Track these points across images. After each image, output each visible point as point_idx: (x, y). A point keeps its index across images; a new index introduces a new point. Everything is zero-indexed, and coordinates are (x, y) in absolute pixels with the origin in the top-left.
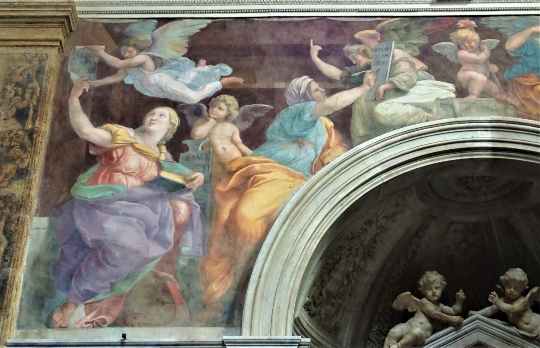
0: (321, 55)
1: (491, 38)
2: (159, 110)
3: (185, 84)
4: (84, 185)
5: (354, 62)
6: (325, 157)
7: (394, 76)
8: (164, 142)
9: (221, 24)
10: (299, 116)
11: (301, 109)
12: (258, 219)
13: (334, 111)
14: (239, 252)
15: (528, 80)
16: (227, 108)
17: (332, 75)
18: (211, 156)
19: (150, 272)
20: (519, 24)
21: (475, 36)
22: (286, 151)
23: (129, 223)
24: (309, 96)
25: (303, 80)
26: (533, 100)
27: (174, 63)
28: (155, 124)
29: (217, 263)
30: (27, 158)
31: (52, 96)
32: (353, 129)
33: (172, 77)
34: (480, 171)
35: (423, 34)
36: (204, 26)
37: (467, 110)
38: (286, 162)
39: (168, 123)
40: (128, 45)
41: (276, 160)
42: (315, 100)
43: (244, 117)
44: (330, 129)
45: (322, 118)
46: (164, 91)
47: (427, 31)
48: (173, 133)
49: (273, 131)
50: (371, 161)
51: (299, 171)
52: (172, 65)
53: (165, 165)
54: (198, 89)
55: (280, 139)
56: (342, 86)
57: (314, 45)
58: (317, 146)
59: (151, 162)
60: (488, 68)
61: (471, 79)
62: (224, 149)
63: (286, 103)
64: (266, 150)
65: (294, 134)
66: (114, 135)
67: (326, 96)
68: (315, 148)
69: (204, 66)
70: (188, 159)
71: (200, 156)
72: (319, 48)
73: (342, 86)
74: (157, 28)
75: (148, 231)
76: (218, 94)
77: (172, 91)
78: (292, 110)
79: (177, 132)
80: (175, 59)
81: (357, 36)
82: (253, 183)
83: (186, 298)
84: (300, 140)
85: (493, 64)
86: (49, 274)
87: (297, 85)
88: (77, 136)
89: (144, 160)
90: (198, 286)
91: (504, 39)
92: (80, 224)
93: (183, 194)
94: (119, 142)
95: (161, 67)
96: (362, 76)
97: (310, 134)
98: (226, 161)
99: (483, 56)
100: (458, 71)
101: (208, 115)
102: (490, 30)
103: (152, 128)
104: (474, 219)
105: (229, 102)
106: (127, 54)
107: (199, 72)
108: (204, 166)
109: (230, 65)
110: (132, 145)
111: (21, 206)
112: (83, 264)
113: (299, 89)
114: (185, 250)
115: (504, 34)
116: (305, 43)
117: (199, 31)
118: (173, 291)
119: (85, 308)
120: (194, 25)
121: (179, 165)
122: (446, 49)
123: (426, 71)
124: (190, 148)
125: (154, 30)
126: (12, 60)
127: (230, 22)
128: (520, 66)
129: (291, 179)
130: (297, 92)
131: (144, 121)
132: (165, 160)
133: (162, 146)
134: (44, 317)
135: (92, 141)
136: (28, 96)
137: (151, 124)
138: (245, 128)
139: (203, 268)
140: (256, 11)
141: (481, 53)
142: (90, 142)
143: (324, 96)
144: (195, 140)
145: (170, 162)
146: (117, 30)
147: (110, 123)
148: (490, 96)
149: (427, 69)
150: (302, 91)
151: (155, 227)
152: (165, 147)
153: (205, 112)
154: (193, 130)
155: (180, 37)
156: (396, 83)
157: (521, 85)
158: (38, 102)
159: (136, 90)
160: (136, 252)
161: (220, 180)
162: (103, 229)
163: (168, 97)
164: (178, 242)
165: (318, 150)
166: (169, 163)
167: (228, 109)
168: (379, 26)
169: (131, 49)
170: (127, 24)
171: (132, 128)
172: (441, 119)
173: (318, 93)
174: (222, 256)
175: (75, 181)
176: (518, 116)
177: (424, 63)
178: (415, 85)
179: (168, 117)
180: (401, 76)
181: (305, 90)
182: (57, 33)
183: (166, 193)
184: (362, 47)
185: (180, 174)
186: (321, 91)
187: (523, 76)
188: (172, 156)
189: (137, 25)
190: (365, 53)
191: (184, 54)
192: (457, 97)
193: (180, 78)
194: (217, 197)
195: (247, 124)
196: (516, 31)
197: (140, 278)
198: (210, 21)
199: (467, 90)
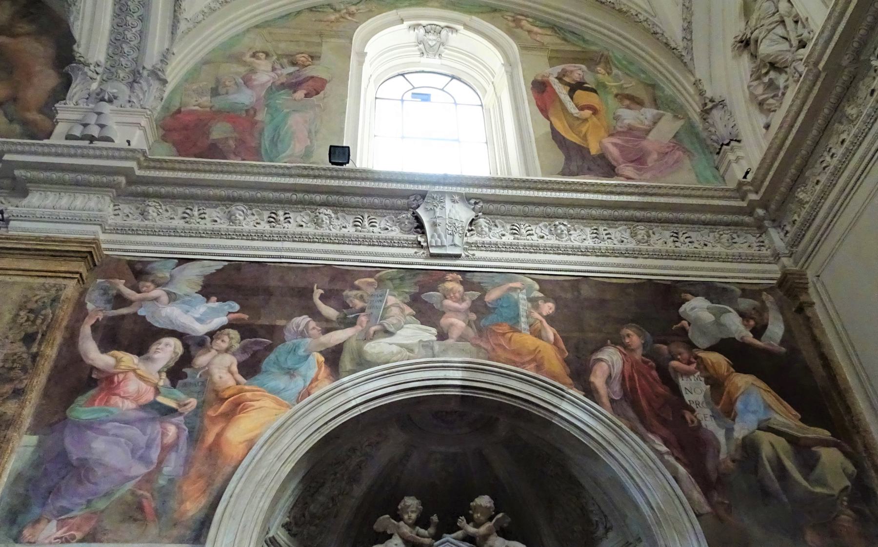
0: (322, 298)
2: (165, 340)
3: (194, 318)
4: (81, 406)
5: (351, 306)
6: (312, 388)
7: (385, 319)
8: (165, 370)
12: (240, 443)
14: (218, 473)
19: (130, 490)
20: (498, 279)
21: (460, 288)
23: (118, 444)
26: (503, 345)
27: (187, 298)
29: (194, 483)
30: (26, 379)
31: (64, 323)
32: (341, 364)
34: (453, 406)
35: (416, 284)
36: (220, 267)
37: (444, 352)
38: (275, 392)
40: (147, 281)
43: (244, 349)
45: (315, 353)
46: (173, 324)
47: (419, 281)
49: (267, 363)
50: (352, 393)
51: (286, 400)
53: (162, 390)
56: (338, 326)
57: (317, 288)
59: (149, 387)
61: (452, 325)
62: (221, 378)
65: (286, 366)
66: (118, 361)
72: (321, 291)
73: (338, 326)
75: (133, 452)
76: (223, 328)
81: (357, 282)
82: (243, 409)
83: (158, 514)
86: (28, 491)
88: (82, 360)
89: (143, 386)
90: (173, 504)
91: (484, 292)
92: (69, 443)
93: (174, 417)
94: (123, 367)
96: (356, 317)
98: (220, 389)
99: (465, 305)
102: (473, 283)
103: (156, 356)
104: (452, 450)
105: (232, 336)
106: (144, 289)
109: (239, 304)
110: (134, 371)
111: (10, 425)
112: (64, 481)
113: (298, 326)
114: (166, 470)
116: (310, 287)
118: (148, 509)
119: (57, 526)
121: (175, 391)
124: (188, 376)
126: (31, 288)
127: (244, 265)
128: (496, 316)
129: (278, 407)
134: (15, 531)
135: (97, 366)
136: (39, 321)
139: (180, 487)
140: (268, 257)
142: (95, 367)
146: (139, 267)
147: (118, 350)
148: (466, 340)
150: (301, 328)
151: (143, 448)
153: (209, 344)
155: (197, 275)
156: (386, 325)
157: (494, 331)
158: (48, 327)
160: (120, 470)
161: (211, 406)
162: (90, 448)
163: (176, 329)
164: (161, 462)
168: (378, 275)
169: (148, 284)
170: (149, 262)
173: (315, 331)
174: (200, 476)
175: (72, 402)
176: (489, 359)
178: (402, 327)
180: (390, 319)
182: (81, 267)
183: (158, 416)
184: (359, 293)
185: (176, 400)
187: (497, 325)
189: (159, 264)
190: (361, 298)
192: (437, 340)
194: (206, 422)
196: (496, 286)
197: (117, 495)
198: (226, 263)
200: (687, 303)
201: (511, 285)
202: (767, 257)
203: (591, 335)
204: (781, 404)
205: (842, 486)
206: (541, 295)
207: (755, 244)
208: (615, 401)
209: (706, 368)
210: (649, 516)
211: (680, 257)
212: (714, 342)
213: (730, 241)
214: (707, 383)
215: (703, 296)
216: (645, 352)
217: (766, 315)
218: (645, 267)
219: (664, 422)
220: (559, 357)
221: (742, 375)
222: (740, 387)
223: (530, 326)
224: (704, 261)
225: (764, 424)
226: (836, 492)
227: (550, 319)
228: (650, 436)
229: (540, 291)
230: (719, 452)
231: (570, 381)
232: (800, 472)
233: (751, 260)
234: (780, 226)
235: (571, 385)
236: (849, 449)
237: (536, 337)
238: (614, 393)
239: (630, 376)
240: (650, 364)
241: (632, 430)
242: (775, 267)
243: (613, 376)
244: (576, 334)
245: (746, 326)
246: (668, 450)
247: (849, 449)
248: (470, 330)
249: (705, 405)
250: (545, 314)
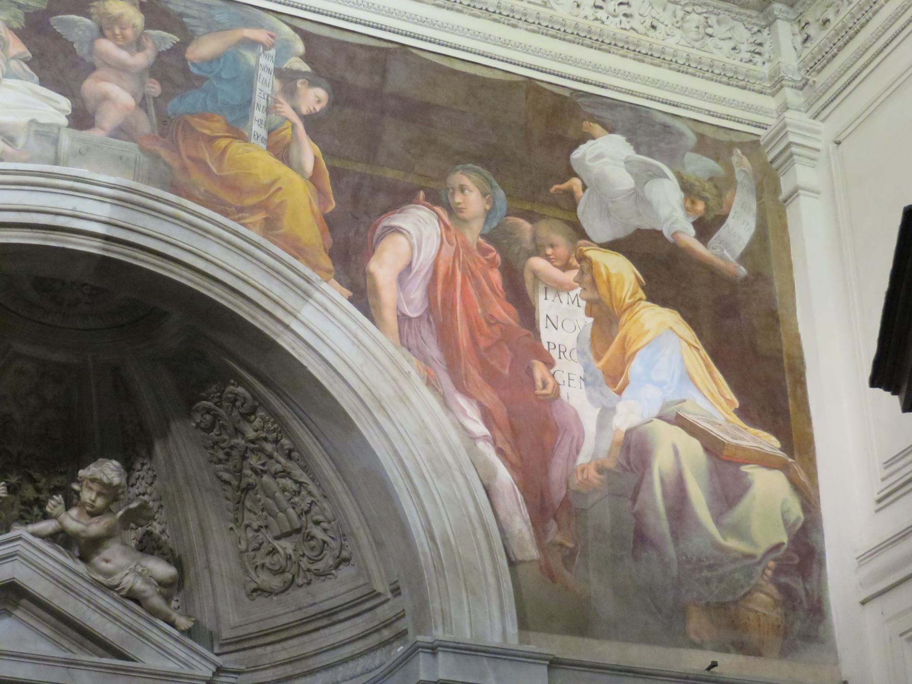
1: (165, 30)
15: (207, 123)
21: (138, 19)
26: (206, 164)
37: (80, 155)
60: (143, 84)
85: (153, 80)
91: (187, 37)
99: (141, 60)
100: (85, 79)
102: (166, 13)
104: (58, 357)
115: (189, 28)
122: (76, 30)
123: (26, 63)
128: (203, 95)
141: (140, 54)
148: (130, 138)
149: (28, 60)
157: (193, 130)
172: (26, 162)
177: (26, 46)
192: (69, 126)
196: (214, 28)
199: (92, 117)
200: (590, 142)
201: (249, 33)
202: (761, 79)
203: (390, 174)
204: (711, 374)
205: (775, 541)
206: (305, 68)
207: (744, 47)
208: (410, 319)
209: (593, 283)
210: (425, 554)
211: (599, 43)
212: (620, 233)
213: (701, 30)
214: (589, 313)
215: (623, 134)
216: (487, 230)
217: (729, 195)
218: (526, 50)
219: (492, 377)
220: (316, 207)
221: (657, 309)
222: (648, 331)
223: (269, 132)
224: (642, 61)
225: (673, 409)
226: (760, 552)
227: (313, 123)
228: (462, 401)
229: (307, 58)
230: (578, 452)
231: (326, 263)
232: (711, 508)
233: (730, 78)
234: (799, 21)
235: (329, 272)
236: (803, 477)
237: (276, 156)
238: (409, 303)
239: (447, 273)
240: (491, 255)
241: (428, 383)
242: (770, 103)
243: (416, 267)
244: (360, 168)
245: (687, 210)
246: (486, 432)
247: (803, 477)
248: (142, 116)
249: (575, 354)
250: (304, 110)
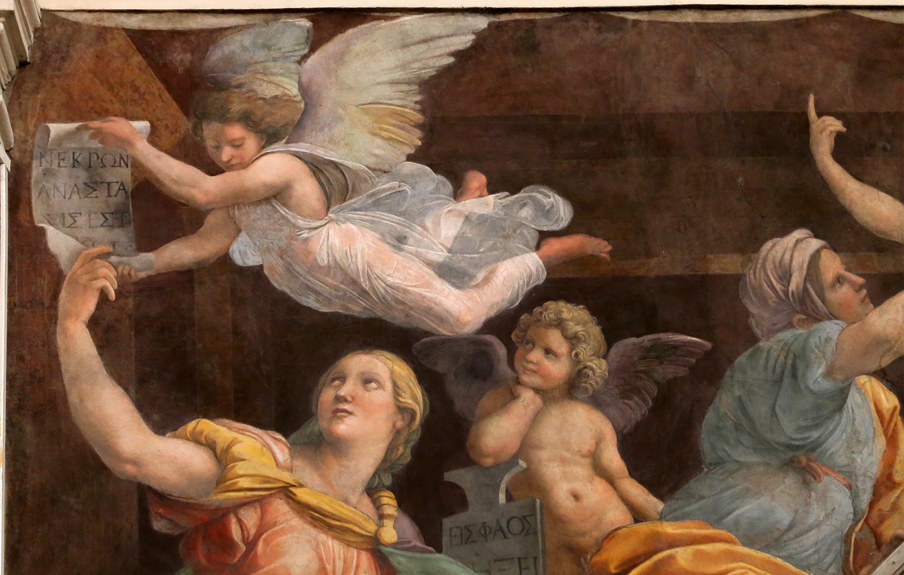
3: (430, 264)
8: (388, 480)
9: (521, 33)
10: (794, 376)
11: (796, 348)
13: (897, 356)
16: (571, 350)
17: (882, 226)
18: (539, 526)
22: (764, 501)
24: (819, 302)
25: (795, 246)
27: (385, 185)
28: (350, 413)
33: (383, 238)
36: (464, 41)
39: (392, 409)
40: (225, 118)
41: (737, 530)
42: (836, 318)
44: (890, 420)
45: (863, 379)
46: (364, 292)
48: (412, 444)
52: (379, 192)
54: (473, 283)
55: (742, 459)
58: (857, 480)
62: (576, 497)
63: (749, 328)
64: (703, 498)
65: (783, 439)
67: (867, 300)
68: (850, 487)
69: (481, 196)
70: (467, 536)
71: (504, 524)
72: (834, 125)
74: (313, 50)
77: (389, 289)
78: (769, 352)
79: (422, 438)
80: (386, 168)
84: (804, 461)
87: (777, 260)
95: (344, 201)
97: (831, 440)
98: (586, 541)
101: (514, 375)
105: (575, 328)
107: (467, 218)
108: (519, 559)
109: (565, 193)
113: (785, 276)
117: (451, 60)
120: (432, 39)
124: (470, 498)
125: (305, 57)
127: (548, 26)
130: (778, 287)
131: (314, 402)
132: (396, 543)
133: (382, 494)
137: (337, 414)
138: (634, 422)
143: (863, 301)
144: (485, 469)
145: (414, 549)
152: (391, 494)
153: (503, 367)
154: (474, 428)
159: (274, 288)
163: (379, 312)
165: (861, 494)
166: (410, 554)
167: (573, 353)
169: (236, 131)
171: (278, 430)
173: (844, 291)
179: (389, 386)
181: (805, 280)
186: (852, 284)
188: (417, 529)
191: (412, 151)
193: (411, 241)
195: (637, 404)
